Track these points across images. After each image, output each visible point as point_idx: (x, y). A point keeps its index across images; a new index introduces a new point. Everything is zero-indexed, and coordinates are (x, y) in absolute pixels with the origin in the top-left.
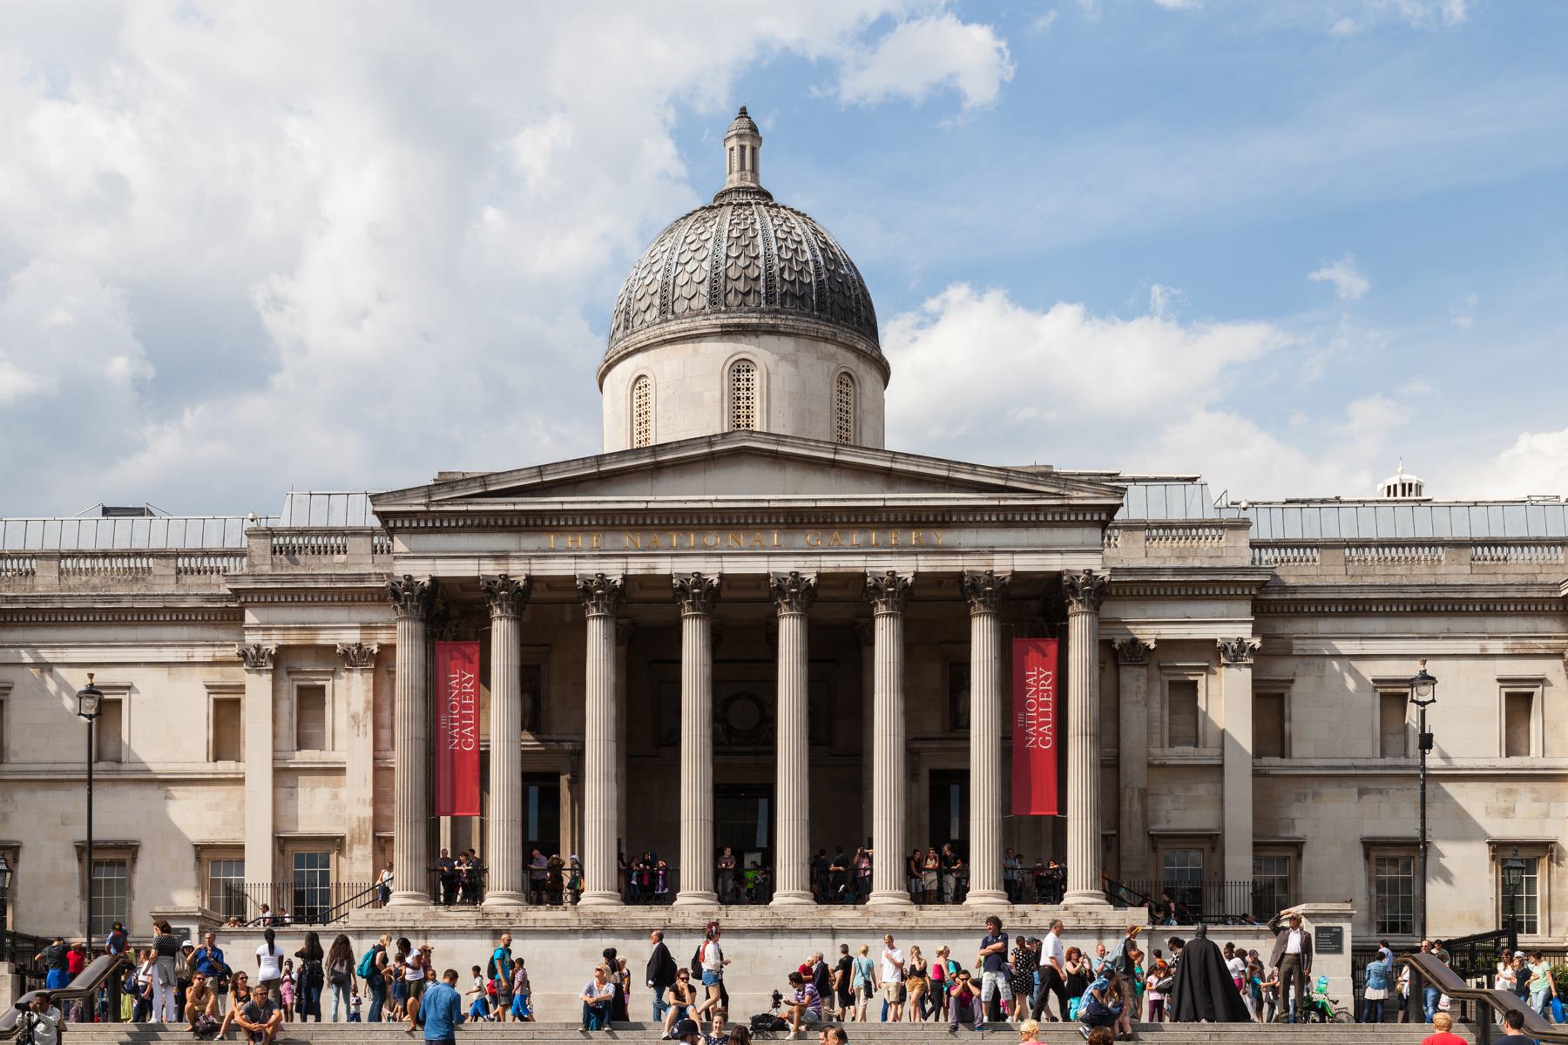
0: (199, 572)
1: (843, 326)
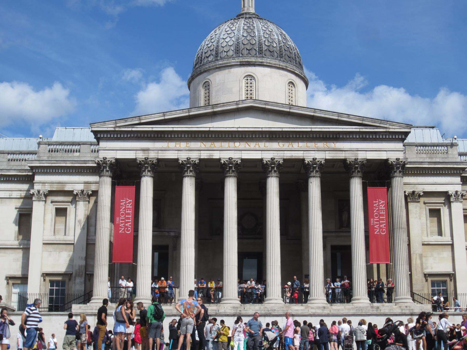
0: (17, 160)
1: (290, 64)
